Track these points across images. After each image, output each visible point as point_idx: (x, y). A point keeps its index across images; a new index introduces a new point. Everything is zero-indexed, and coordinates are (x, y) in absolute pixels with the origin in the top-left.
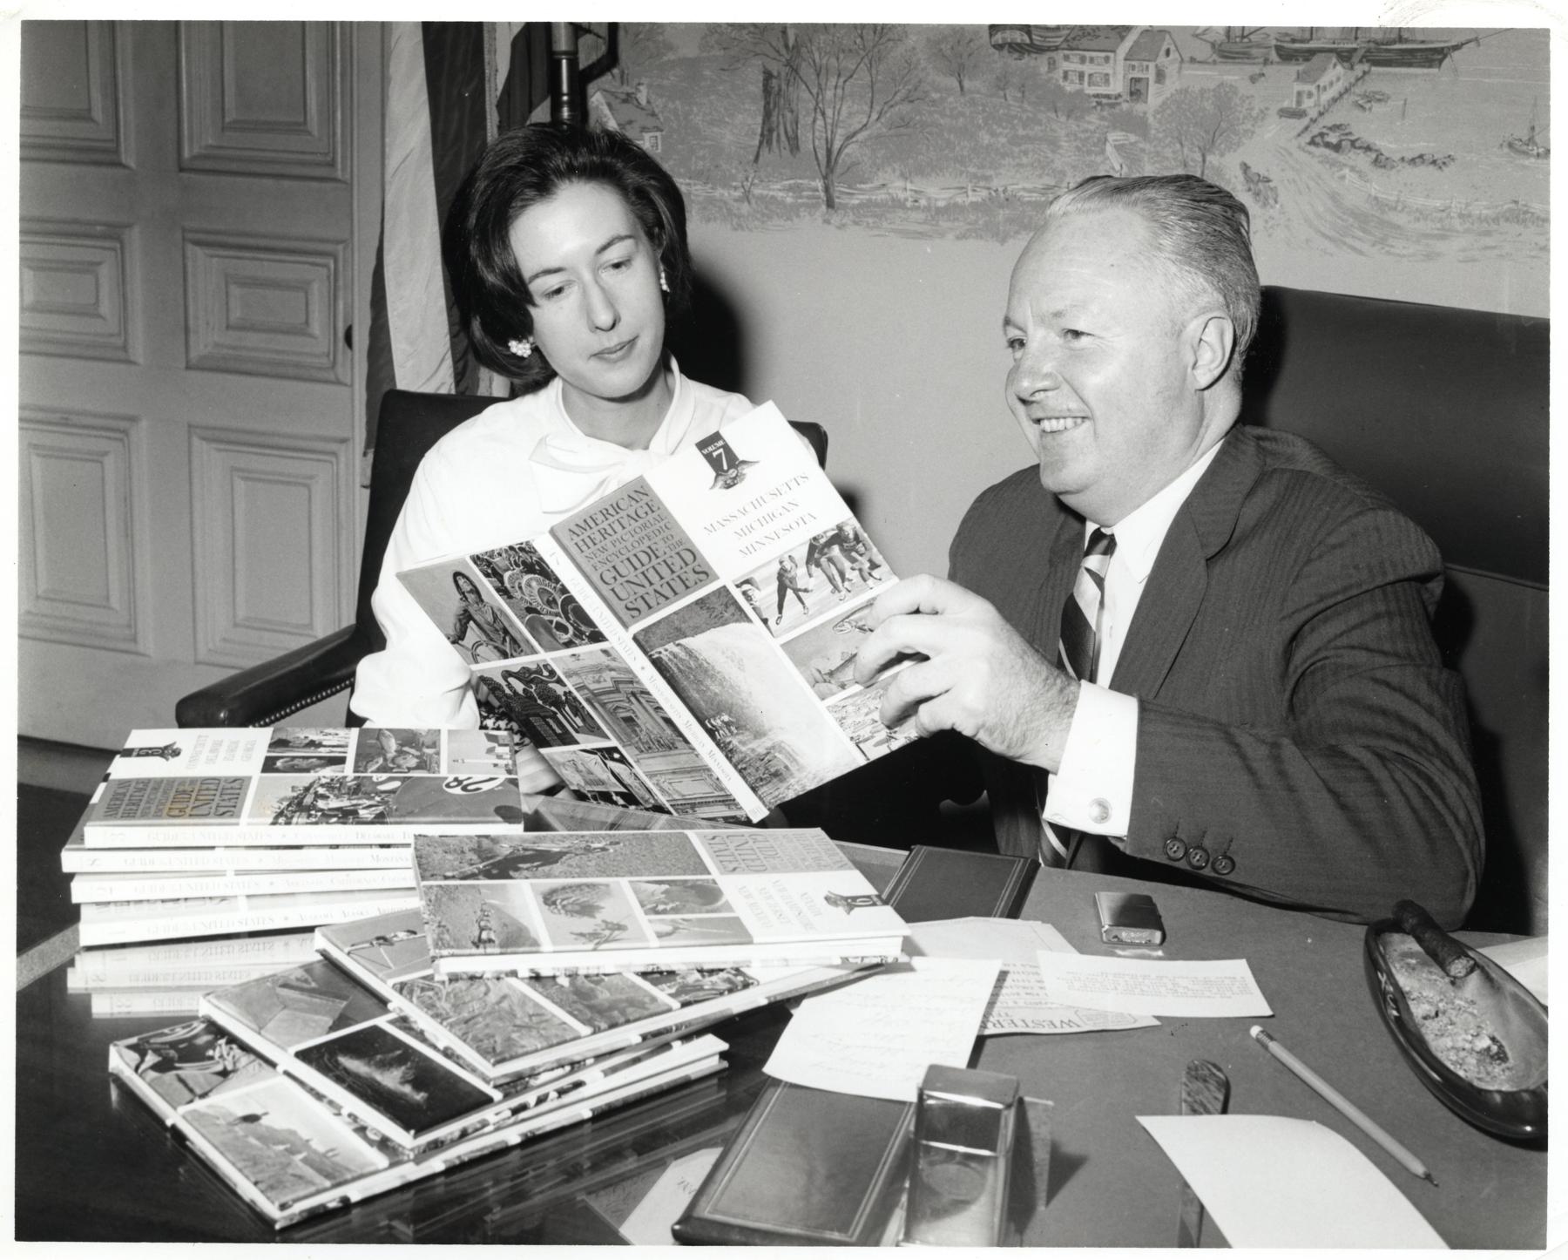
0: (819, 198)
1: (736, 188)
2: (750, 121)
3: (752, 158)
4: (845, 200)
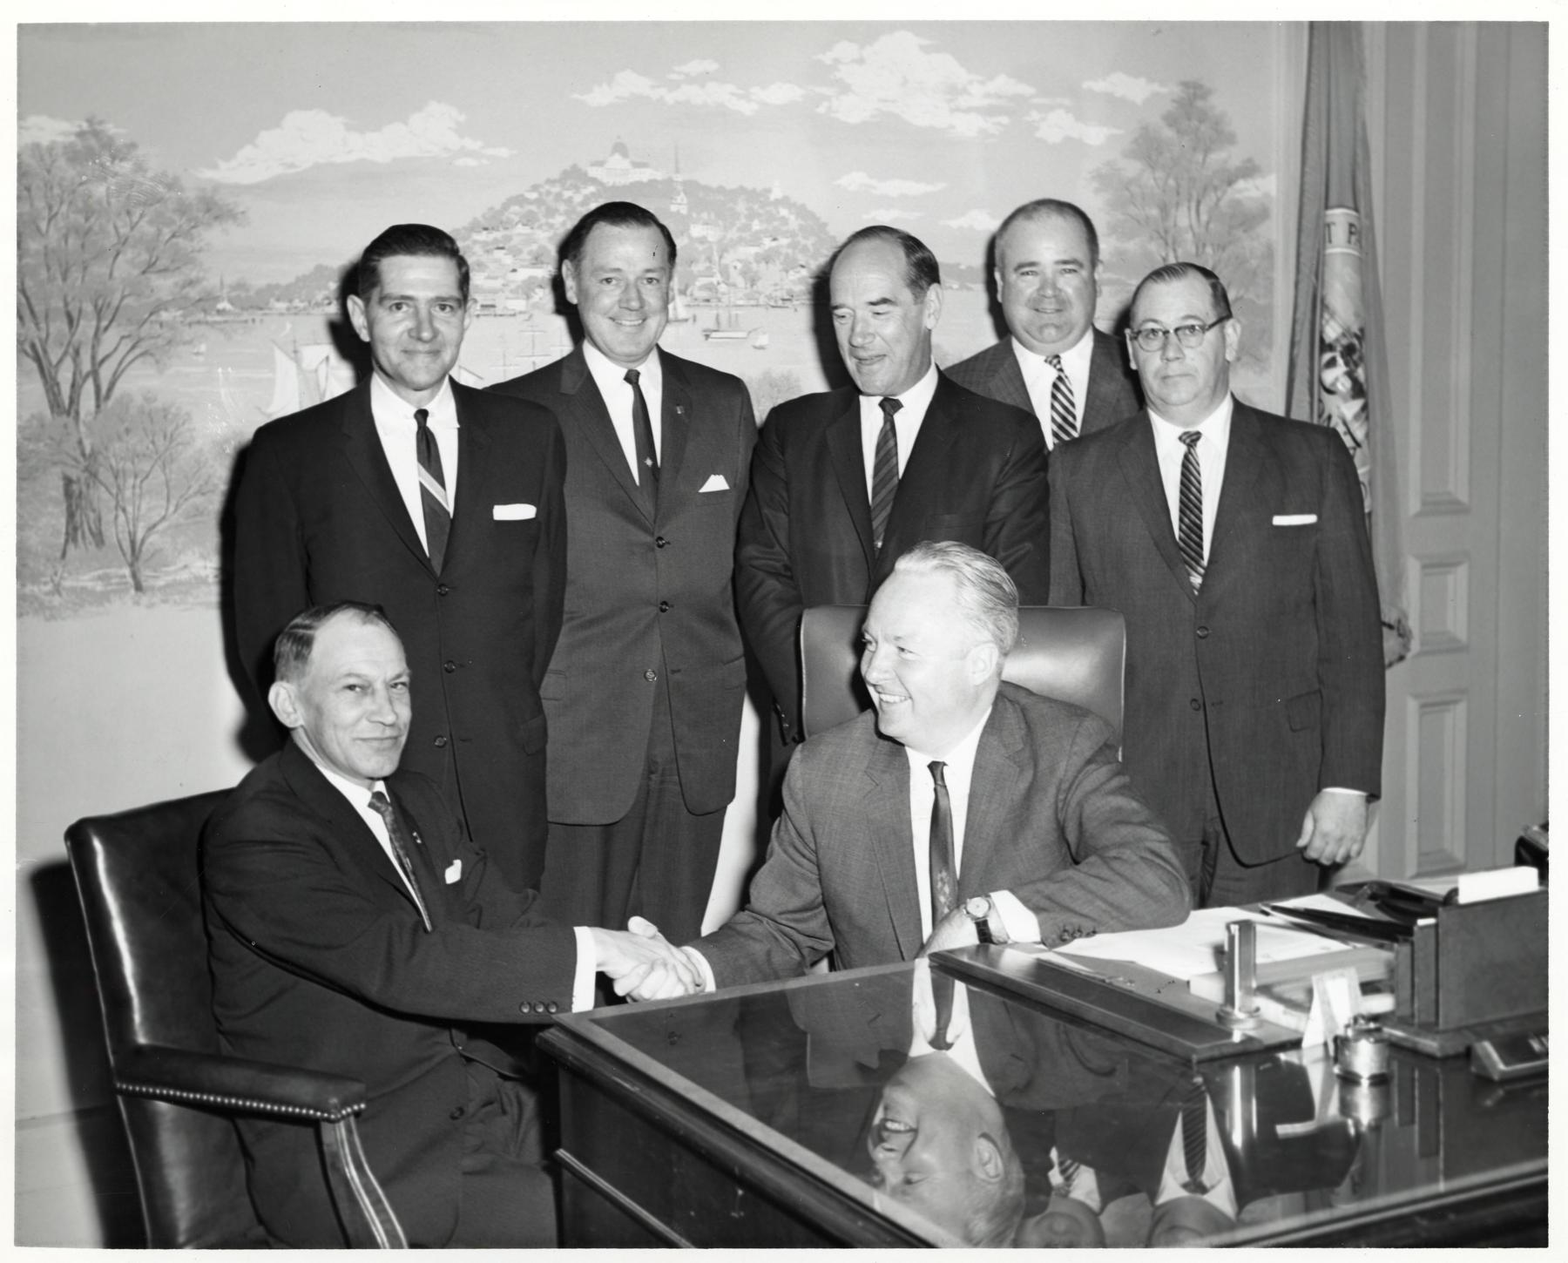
0: (126, 583)
1: (45, 583)
2: (53, 522)
3: (59, 554)
4: (151, 582)
